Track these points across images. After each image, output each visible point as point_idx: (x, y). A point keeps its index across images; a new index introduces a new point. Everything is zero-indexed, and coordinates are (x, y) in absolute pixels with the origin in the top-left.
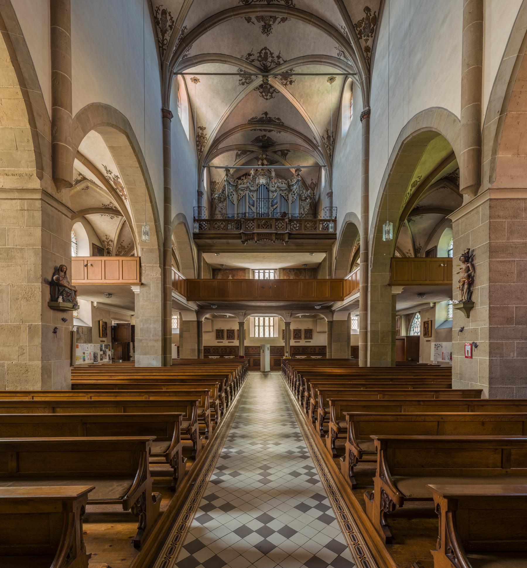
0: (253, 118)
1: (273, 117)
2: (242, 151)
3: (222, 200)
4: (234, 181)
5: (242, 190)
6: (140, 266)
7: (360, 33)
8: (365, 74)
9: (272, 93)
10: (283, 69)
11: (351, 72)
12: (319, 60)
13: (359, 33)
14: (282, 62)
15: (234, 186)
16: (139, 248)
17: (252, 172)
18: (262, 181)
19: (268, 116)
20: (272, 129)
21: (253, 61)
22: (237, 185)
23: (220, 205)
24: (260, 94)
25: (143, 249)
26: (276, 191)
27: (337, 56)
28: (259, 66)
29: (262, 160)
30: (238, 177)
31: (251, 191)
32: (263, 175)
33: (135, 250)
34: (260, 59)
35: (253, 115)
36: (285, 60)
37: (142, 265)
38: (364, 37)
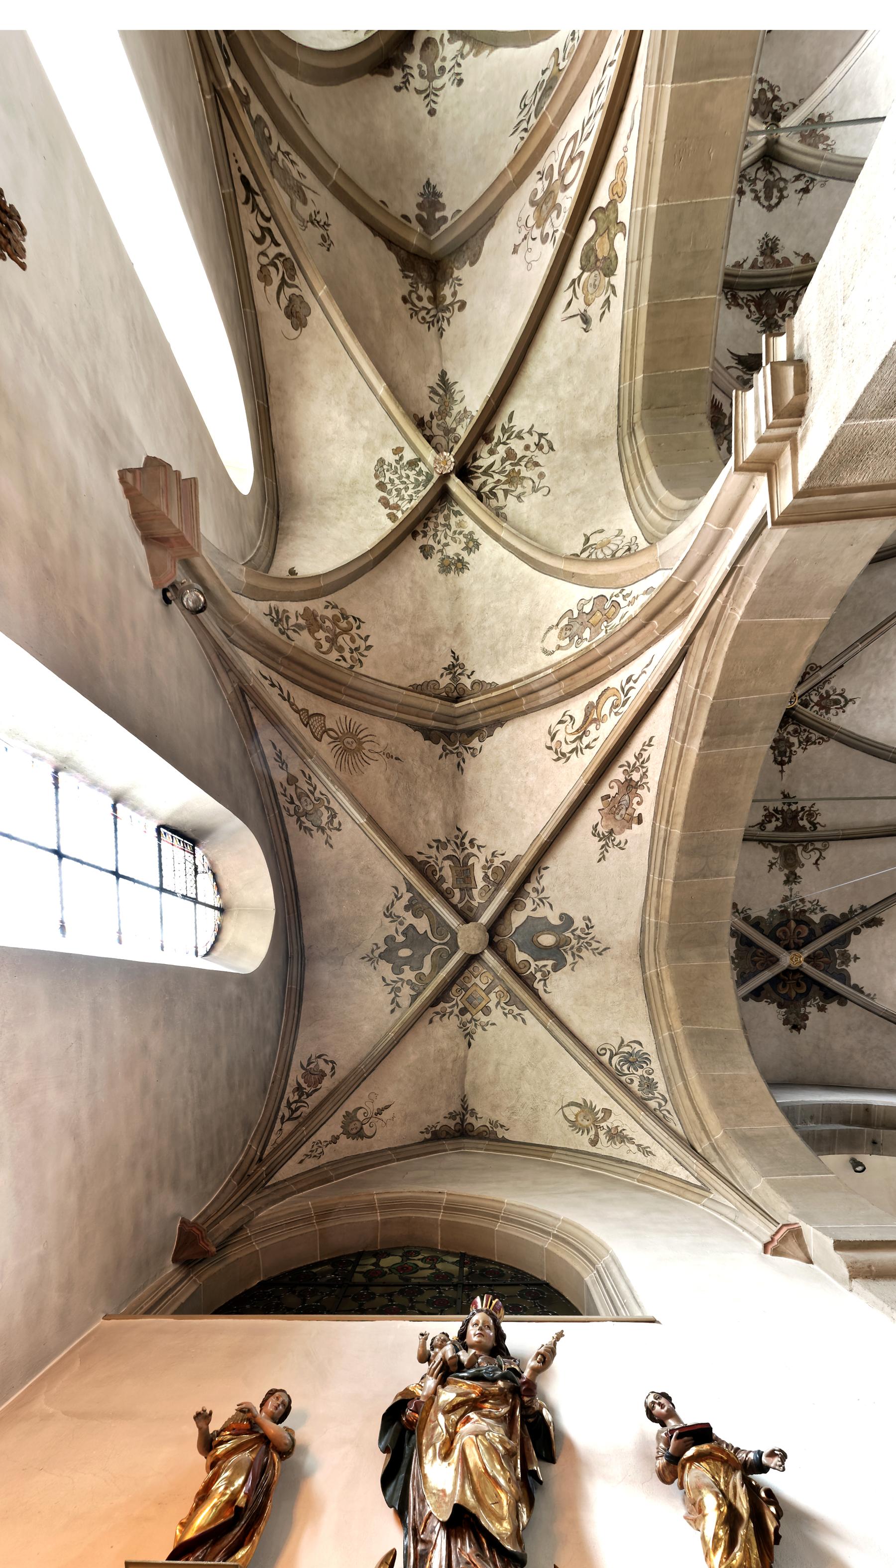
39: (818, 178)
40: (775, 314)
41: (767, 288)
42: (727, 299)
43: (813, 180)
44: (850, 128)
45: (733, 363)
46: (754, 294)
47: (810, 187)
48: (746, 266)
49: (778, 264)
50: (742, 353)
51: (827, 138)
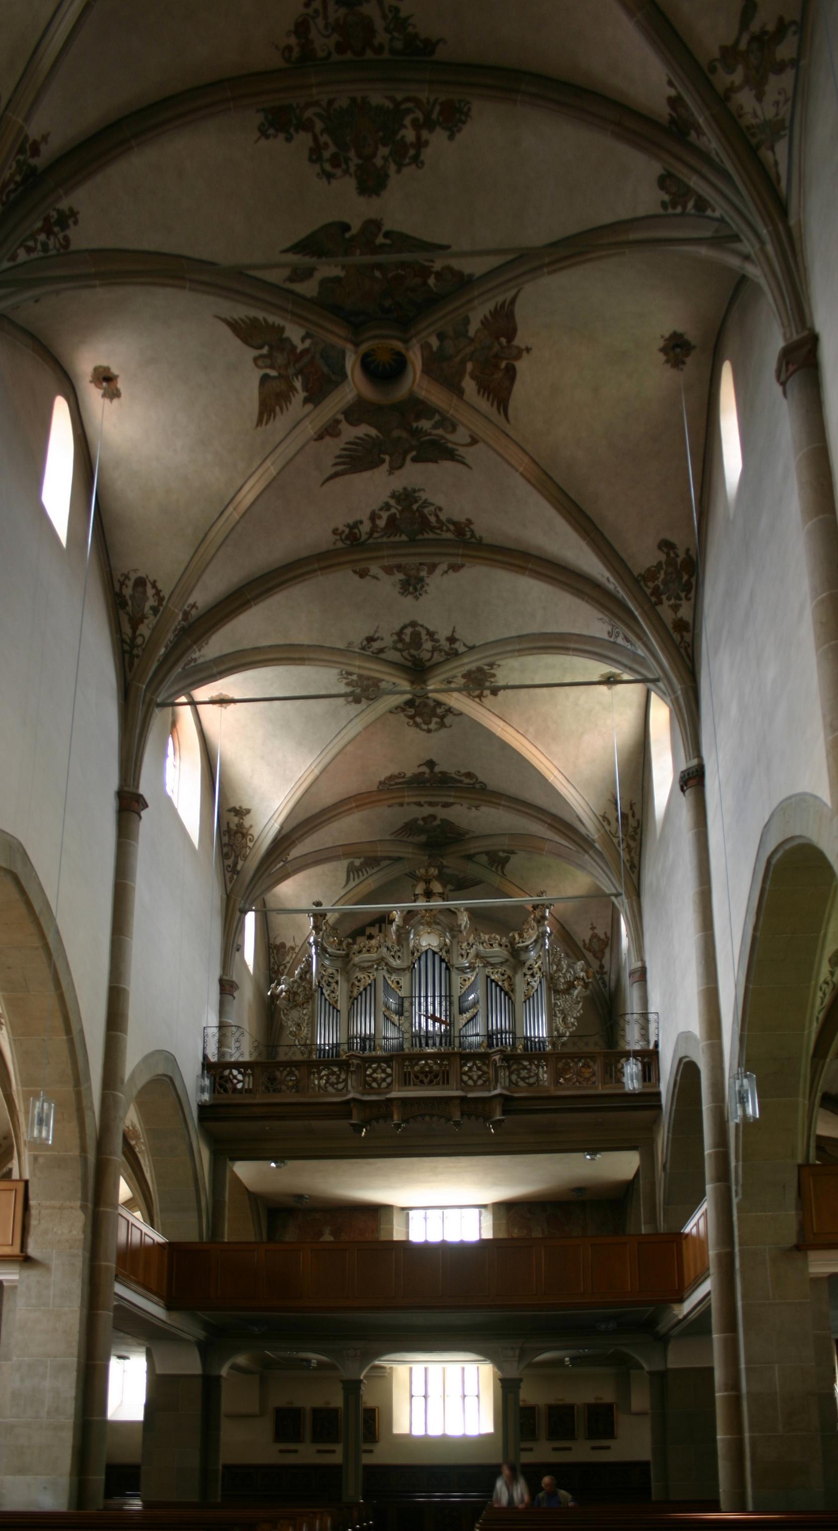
0: (391, 778)
1: (451, 770)
2: (362, 860)
3: (300, 999)
4: (340, 943)
5: (363, 969)
6: (26, 1207)
7: (656, 592)
8: (682, 681)
9: (442, 718)
10: (470, 663)
11: (650, 676)
12: (560, 644)
13: (653, 594)
14: (462, 649)
15: (338, 957)
16: (26, 1155)
17: (397, 916)
18: (428, 940)
19: (437, 769)
20: (452, 800)
21: (381, 651)
22: (347, 955)
23: (295, 1014)
24: (407, 720)
25: (36, 1158)
26: (472, 968)
27: (606, 637)
28: (401, 660)
29: (428, 882)
30: (349, 936)
31: (392, 970)
32: (429, 924)
33: (15, 1162)
34: (400, 646)
35: (393, 769)
36: (470, 644)
37: (32, 1203)
38: (669, 599)
39: (357, 650)
40: (401, 512)
41: (413, 541)
42: (472, 531)
43: (363, 648)
44: (323, 693)
45: (461, 451)
46: (431, 536)
47: (365, 643)
48: (444, 567)
49: (399, 568)
50: (448, 465)
51: (347, 684)
